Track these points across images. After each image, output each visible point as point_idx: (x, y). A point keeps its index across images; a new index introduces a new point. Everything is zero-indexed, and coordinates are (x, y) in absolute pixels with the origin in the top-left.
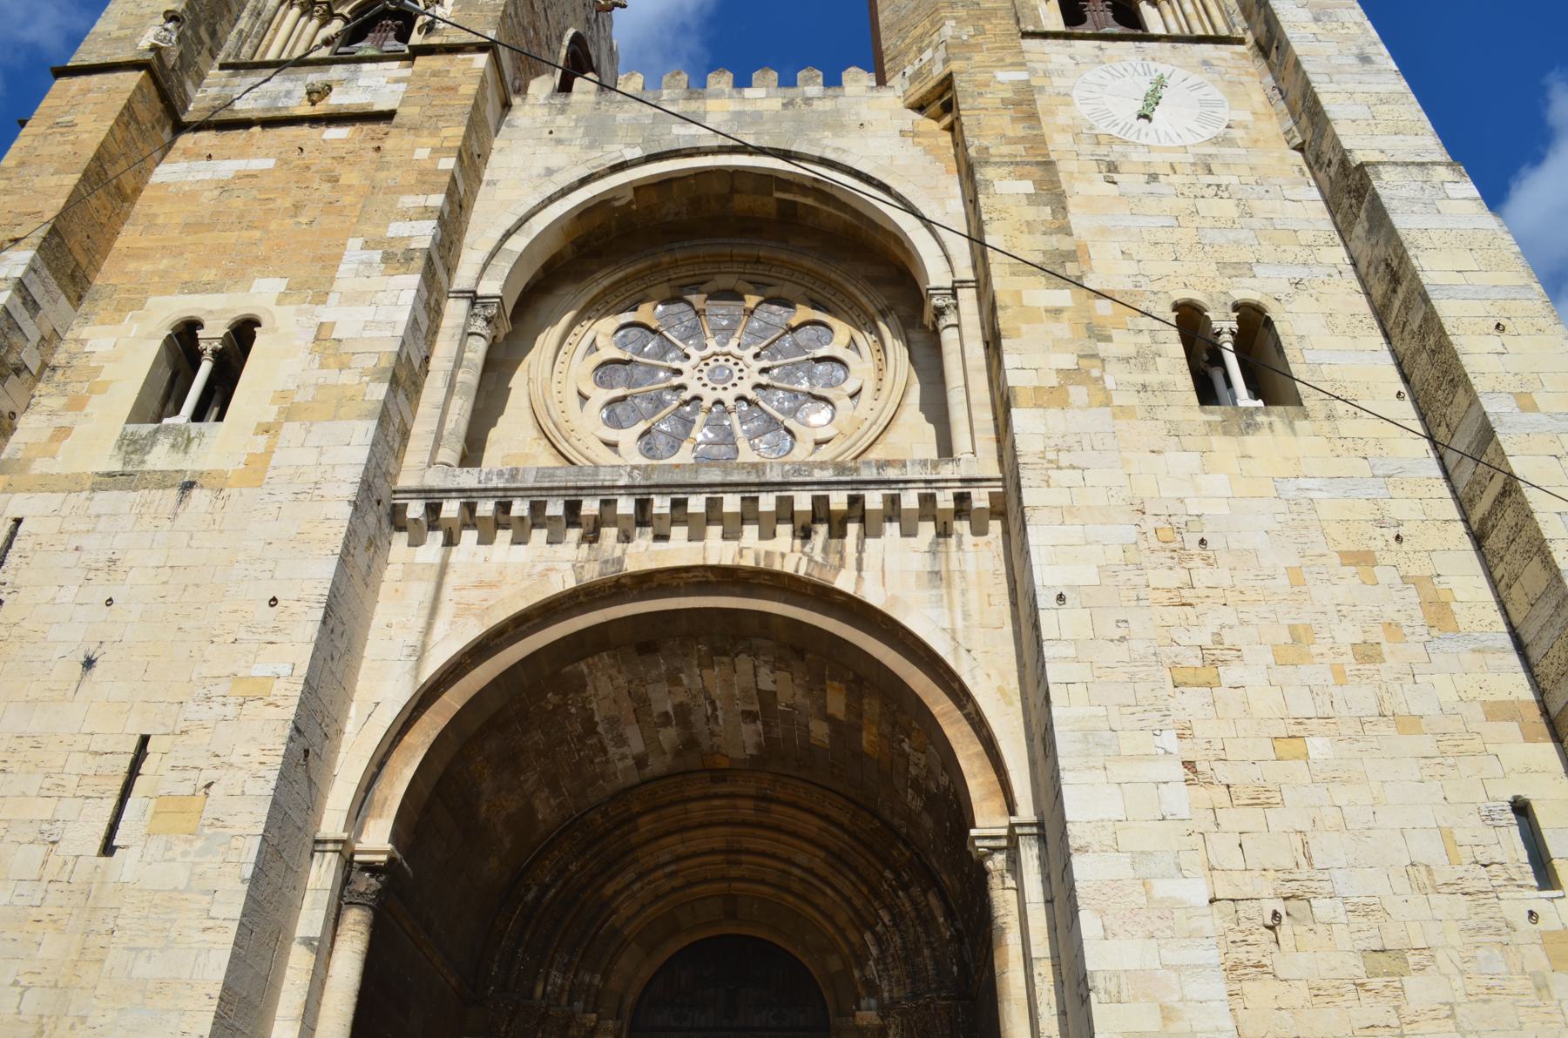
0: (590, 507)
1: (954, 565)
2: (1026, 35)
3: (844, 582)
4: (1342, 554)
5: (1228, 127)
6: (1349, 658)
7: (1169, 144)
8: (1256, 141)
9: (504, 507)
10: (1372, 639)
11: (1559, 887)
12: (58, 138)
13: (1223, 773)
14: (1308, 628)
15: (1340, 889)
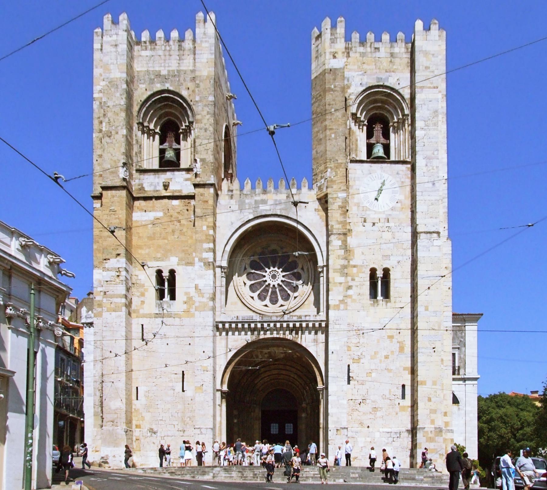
0: (253, 325)
1: (318, 338)
2: (352, 161)
3: (299, 341)
4: (388, 336)
5: (397, 203)
6: (383, 358)
7: (380, 210)
8: (403, 208)
9: (237, 325)
10: (388, 354)
11: (404, 399)
12: (113, 216)
13: (357, 378)
14: (378, 352)
15: (371, 399)
